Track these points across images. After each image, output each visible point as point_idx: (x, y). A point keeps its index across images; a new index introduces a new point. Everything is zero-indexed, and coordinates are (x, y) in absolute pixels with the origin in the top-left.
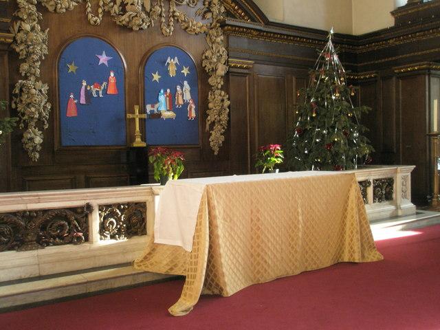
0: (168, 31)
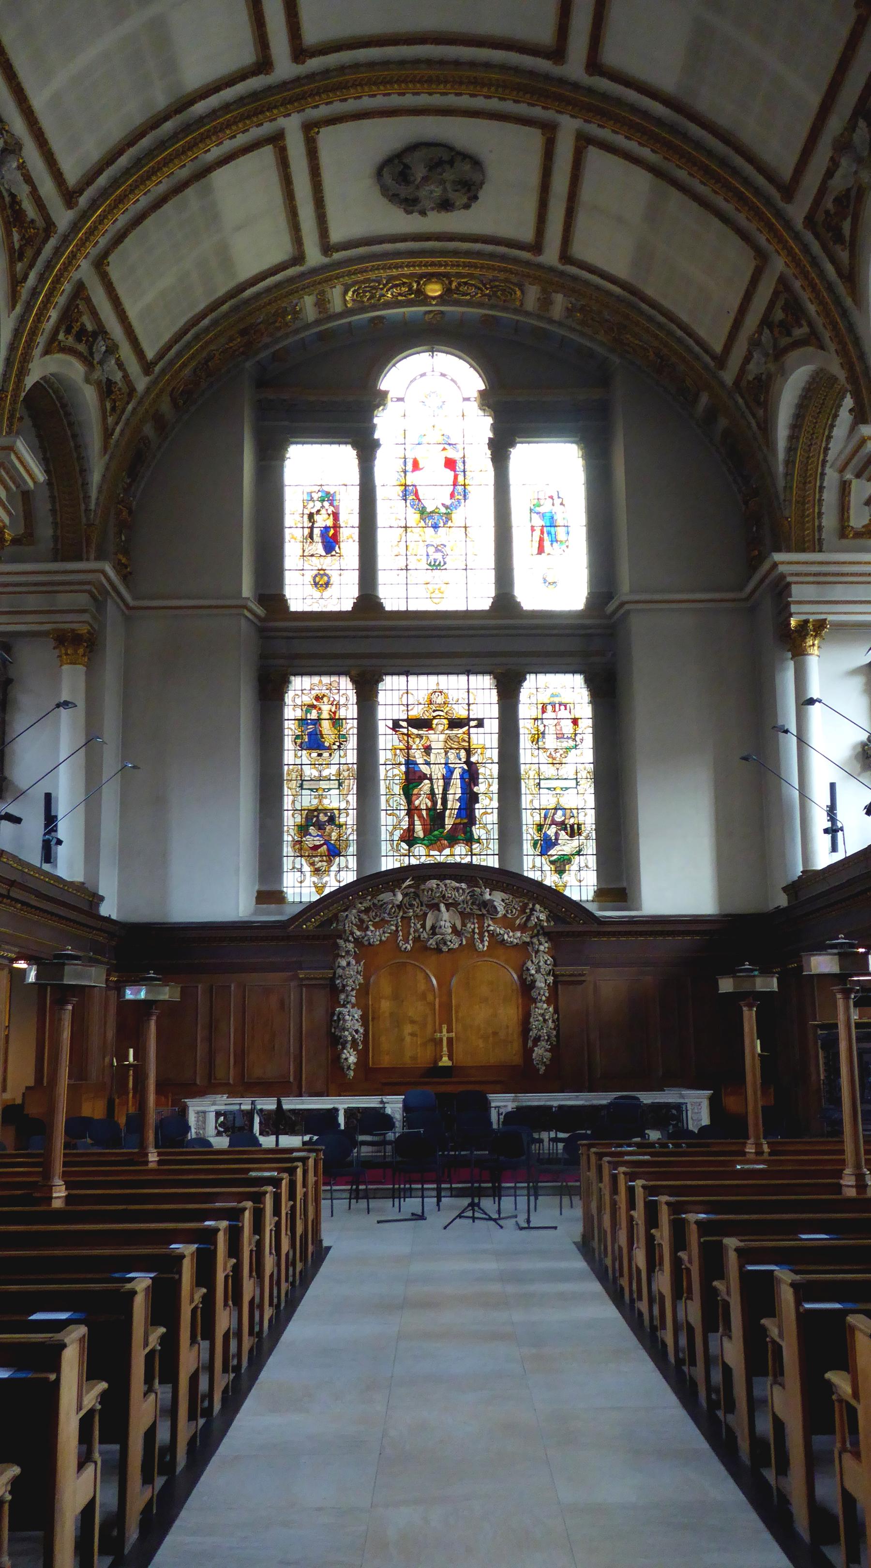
0: (481, 946)
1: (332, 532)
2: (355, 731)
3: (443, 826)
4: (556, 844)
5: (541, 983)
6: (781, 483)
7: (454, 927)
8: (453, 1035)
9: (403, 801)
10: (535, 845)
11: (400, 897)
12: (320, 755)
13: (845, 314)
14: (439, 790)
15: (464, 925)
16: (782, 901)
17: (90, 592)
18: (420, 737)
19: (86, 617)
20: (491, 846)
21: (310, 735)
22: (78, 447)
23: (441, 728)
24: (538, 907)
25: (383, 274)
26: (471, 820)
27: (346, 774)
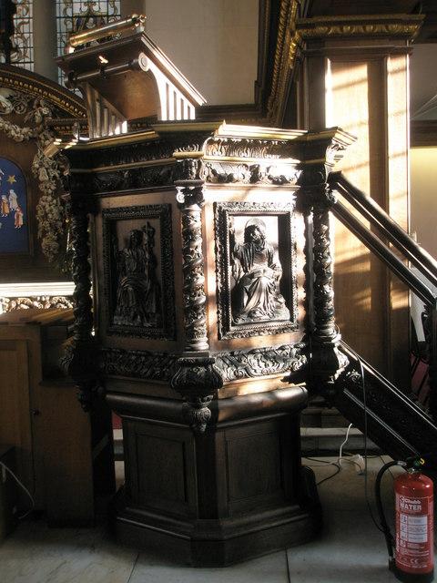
20: (28, 54)
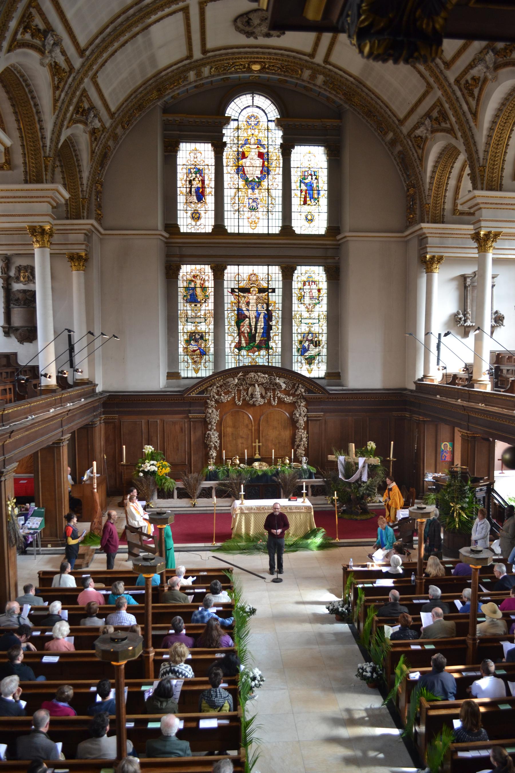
1: (201, 190)
2: (213, 293)
3: (255, 341)
4: (308, 350)
5: (302, 421)
6: (427, 186)
7: (261, 395)
8: (261, 444)
9: (236, 328)
10: (298, 351)
11: (236, 381)
12: (196, 305)
13: (470, 128)
14: (253, 324)
15: (266, 393)
16: (413, 387)
17: (85, 234)
18: (244, 297)
19: (83, 247)
21: (190, 295)
22: (78, 160)
23: (254, 292)
24: (300, 386)
25: (231, 62)
26: (269, 338)
27: (208, 315)
